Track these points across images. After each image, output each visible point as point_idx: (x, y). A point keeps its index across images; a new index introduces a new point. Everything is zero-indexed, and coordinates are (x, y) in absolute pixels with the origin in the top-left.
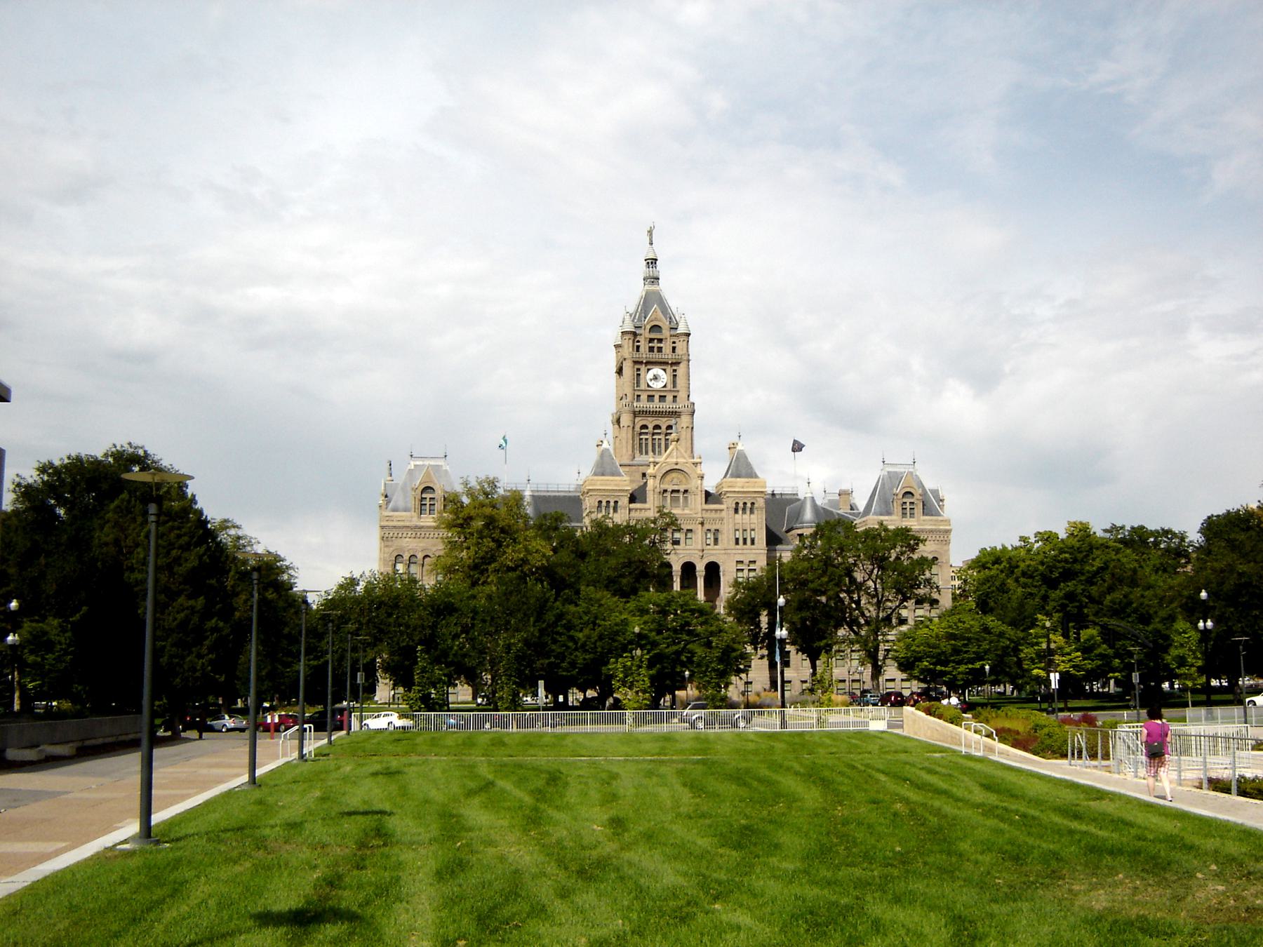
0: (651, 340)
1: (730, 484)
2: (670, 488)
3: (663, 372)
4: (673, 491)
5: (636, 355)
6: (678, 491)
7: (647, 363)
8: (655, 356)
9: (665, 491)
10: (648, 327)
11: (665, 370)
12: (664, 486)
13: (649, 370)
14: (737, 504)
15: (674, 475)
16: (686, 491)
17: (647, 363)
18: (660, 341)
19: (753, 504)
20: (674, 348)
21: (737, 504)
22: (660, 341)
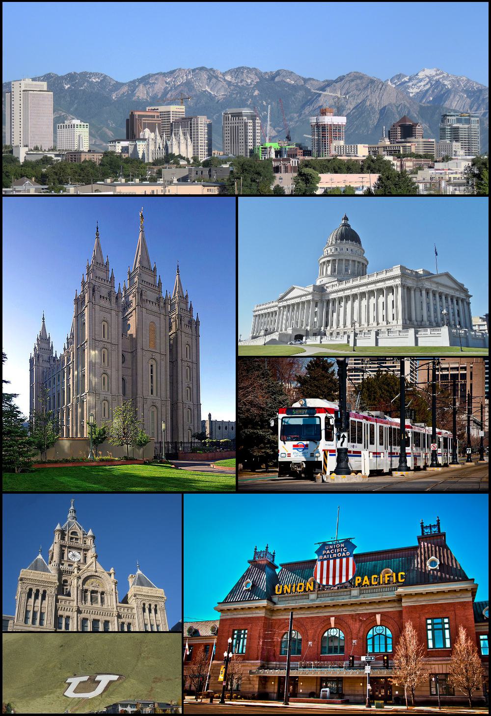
0: (72, 538)
1: (138, 590)
2: (91, 588)
3: (78, 554)
4: (93, 592)
5: (63, 542)
6: (96, 592)
7: (70, 547)
8: (73, 544)
9: (86, 591)
10: (70, 532)
11: (79, 553)
12: (85, 587)
13: (70, 551)
14: (144, 604)
15: (93, 580)
16: (102, 593)
17: (70, 547)
18: (77, 539)
19: (156, 606)
20: (85, 544)
21: (144, 604)
22: (77, 539)
